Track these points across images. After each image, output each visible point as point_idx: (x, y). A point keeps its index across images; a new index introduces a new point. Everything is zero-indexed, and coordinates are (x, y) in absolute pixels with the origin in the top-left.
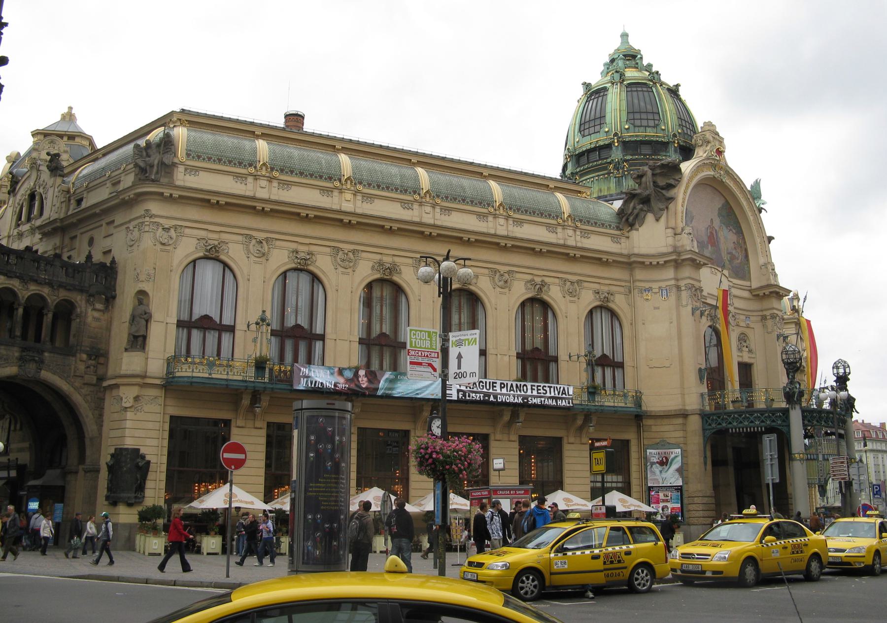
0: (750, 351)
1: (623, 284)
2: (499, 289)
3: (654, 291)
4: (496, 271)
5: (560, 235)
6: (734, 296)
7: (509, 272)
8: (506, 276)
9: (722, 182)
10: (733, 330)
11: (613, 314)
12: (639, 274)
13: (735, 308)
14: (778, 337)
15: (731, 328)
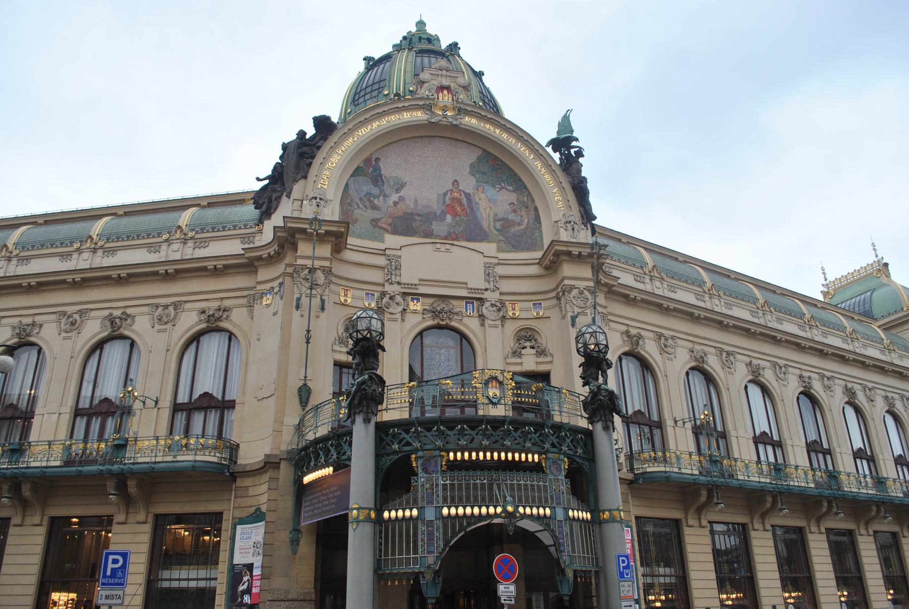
0: (541, 353)
1: (245, 293)
2: (64, 334)
3: (276, 290)
4: (64, 314)
5: (163, 253)
6: (501, 277)
7: (81, 313)
8: (77, 316)
9: (456, 128)
10: (496, 326)
11: (231, 336)
12: (264, 274)
13: (501, 294)
14: (573, 319)
15: (487, 322)
